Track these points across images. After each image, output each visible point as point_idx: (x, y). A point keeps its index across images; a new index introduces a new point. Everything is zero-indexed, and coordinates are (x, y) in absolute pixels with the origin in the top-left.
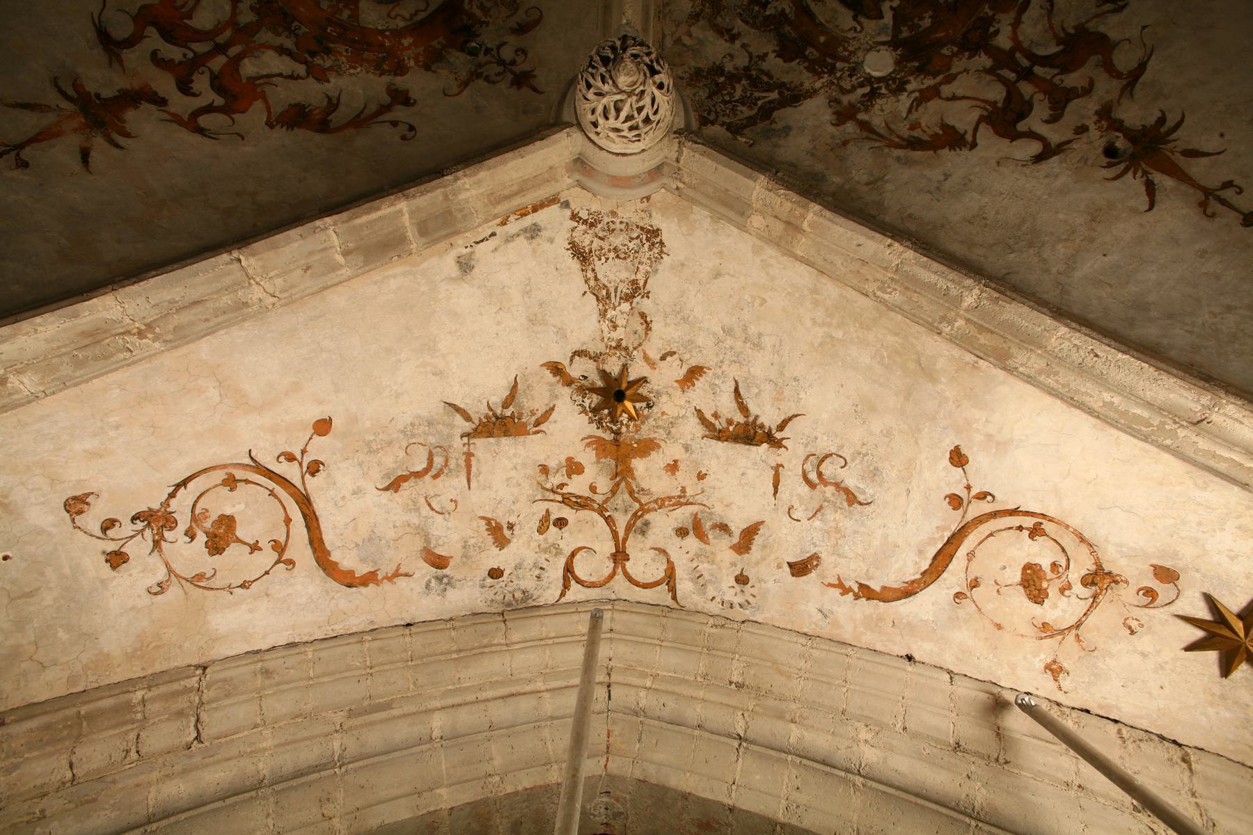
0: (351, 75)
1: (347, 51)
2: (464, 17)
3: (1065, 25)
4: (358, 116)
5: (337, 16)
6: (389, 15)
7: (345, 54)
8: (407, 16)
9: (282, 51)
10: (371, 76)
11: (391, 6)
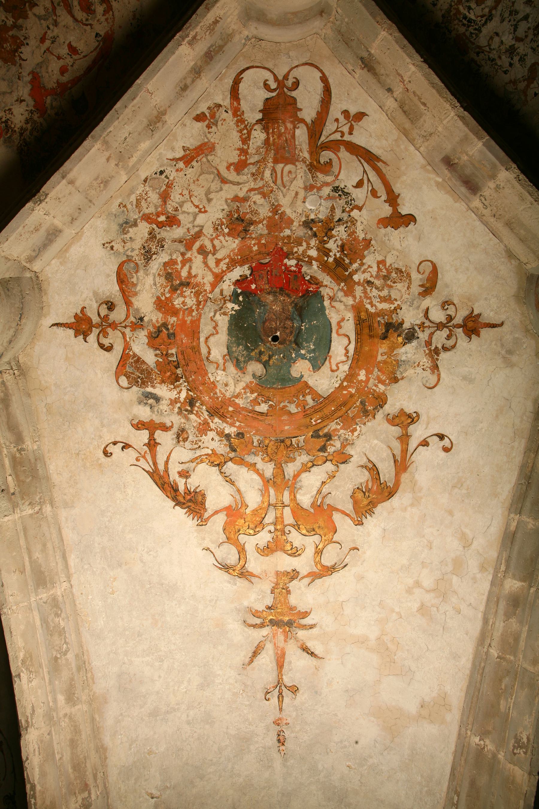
0: (358, 437)
2: (379, 319)
4: (395, 461)
5: (307, 407)
6: (332, 371)
7: (339, 427)
8: (344, 359)
9: (306, 468)
10: (369, 424)
11: (327, 362)
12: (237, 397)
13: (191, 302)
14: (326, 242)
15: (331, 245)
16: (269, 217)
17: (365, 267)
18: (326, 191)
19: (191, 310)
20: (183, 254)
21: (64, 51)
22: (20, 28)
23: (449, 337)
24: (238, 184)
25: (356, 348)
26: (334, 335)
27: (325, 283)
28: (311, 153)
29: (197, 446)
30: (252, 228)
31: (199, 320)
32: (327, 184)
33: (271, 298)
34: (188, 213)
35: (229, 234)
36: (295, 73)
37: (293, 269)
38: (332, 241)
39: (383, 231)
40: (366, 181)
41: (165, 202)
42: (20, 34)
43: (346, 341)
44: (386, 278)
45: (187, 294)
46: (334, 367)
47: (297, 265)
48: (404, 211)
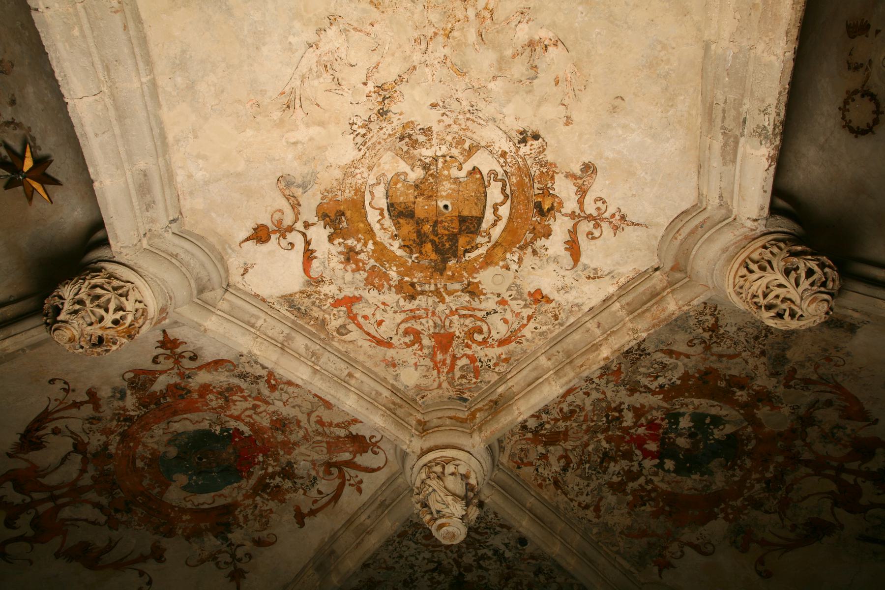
1: (142, 514)
6: (185, 499)
7: (139, 515)
8: (196, 503)
9: (97, 505)
11: (189, 494)
12: (144, 445)
13: (214, 404)
14: (279, 477)
15: (278, 479)
16: (290, 441)
17: (266, 502)
18: (313, 473)
19: (207, 405)
20: (249, 396)
21: (379, 317)
22: (389, 289)
23: (226, 563)
24: (309, 422)
25: (206, 509)
26: (212, 494)
27: (250, 481)
28: (336, 462)
29: (88, 432)
30: (280, 432)
31: (201, 411)
32: (317, 473)
33: (231, 451)
34: (281, 396)
35: (272, 420)
36: (381, 453)
37: (256, 460)
38: (280, 479)
39: (292, 509)
40: (322, 496)
41: (285, 383)
42: (385, 289)
43: (210, 502)
44: (261, 516)
45: (220, 401)
46: (187, 499)
47: (259, 462)
48: (306, 520)
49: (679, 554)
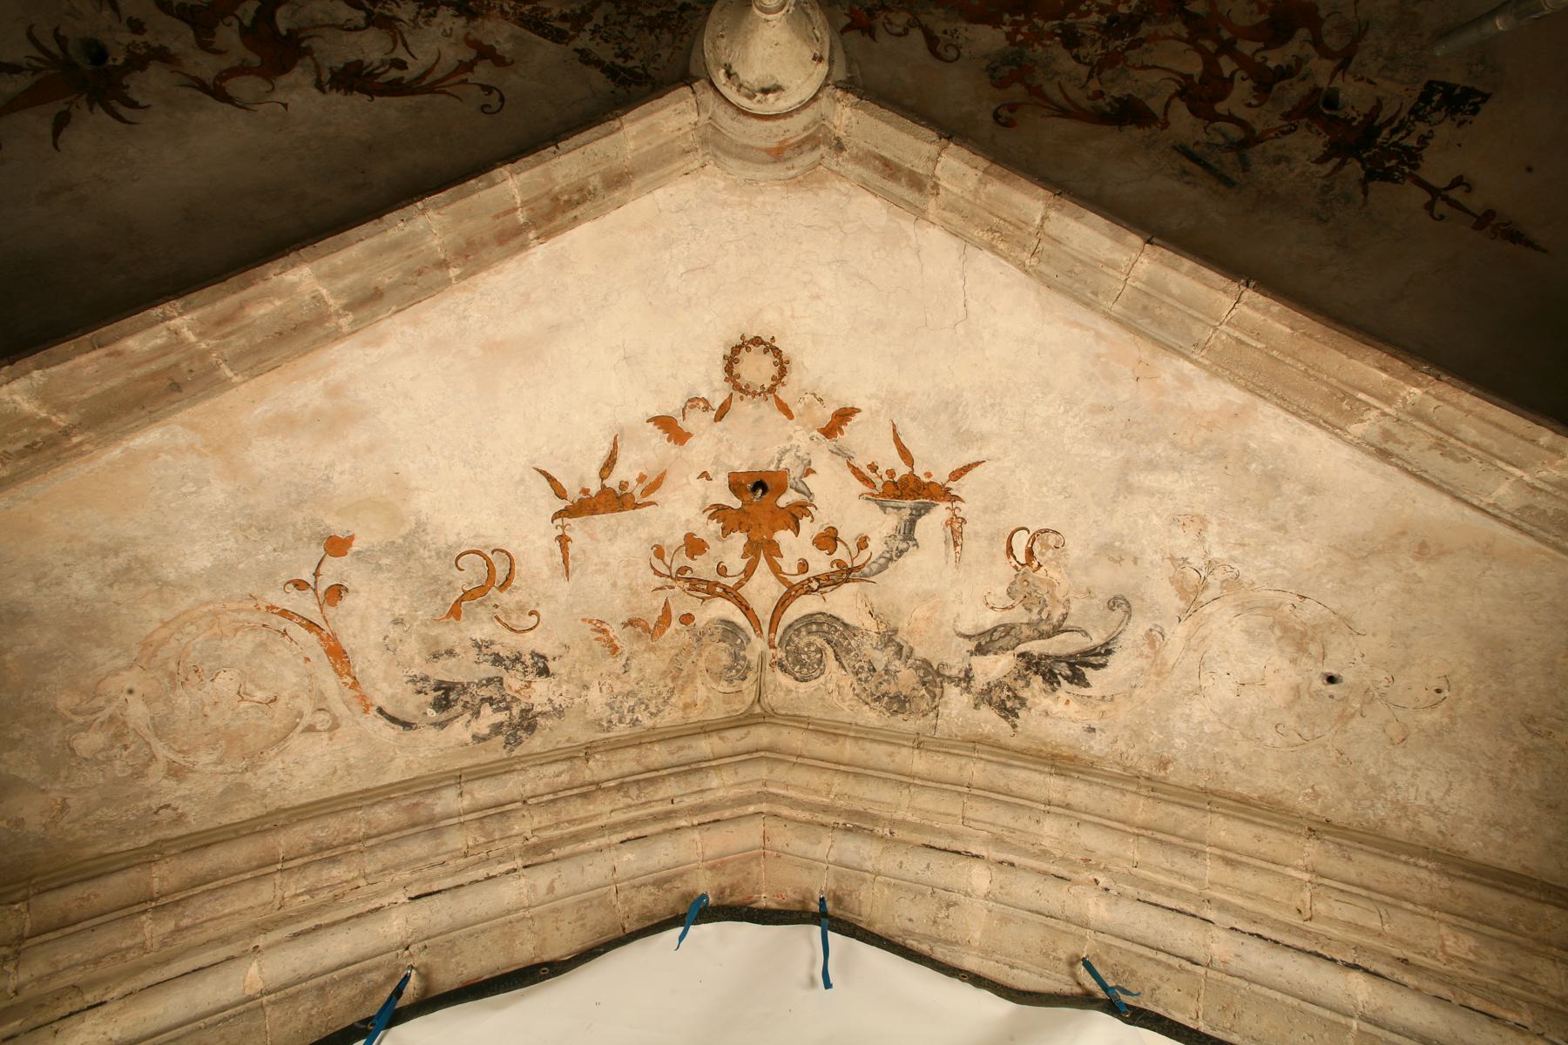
3: (315, 39)
49: (900, 30)
